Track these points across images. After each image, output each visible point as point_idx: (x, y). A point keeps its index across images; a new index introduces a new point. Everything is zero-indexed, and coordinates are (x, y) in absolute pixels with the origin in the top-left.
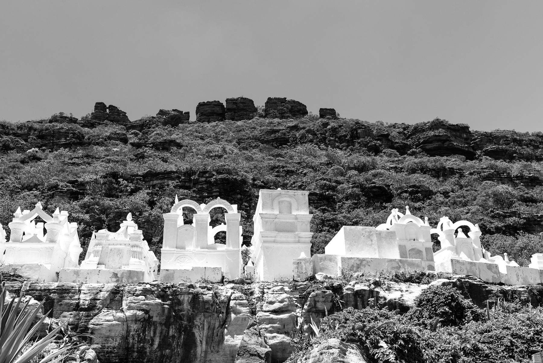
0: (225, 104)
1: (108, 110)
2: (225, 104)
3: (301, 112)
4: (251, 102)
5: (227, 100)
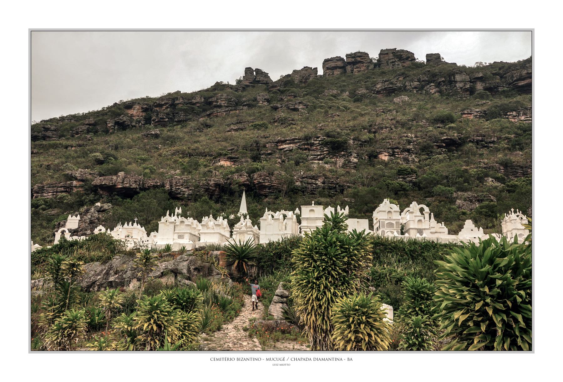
0: (345, 58)
1: (254, 73)
2: (345, 58)
3: (410, 59)
5: (347, 55)
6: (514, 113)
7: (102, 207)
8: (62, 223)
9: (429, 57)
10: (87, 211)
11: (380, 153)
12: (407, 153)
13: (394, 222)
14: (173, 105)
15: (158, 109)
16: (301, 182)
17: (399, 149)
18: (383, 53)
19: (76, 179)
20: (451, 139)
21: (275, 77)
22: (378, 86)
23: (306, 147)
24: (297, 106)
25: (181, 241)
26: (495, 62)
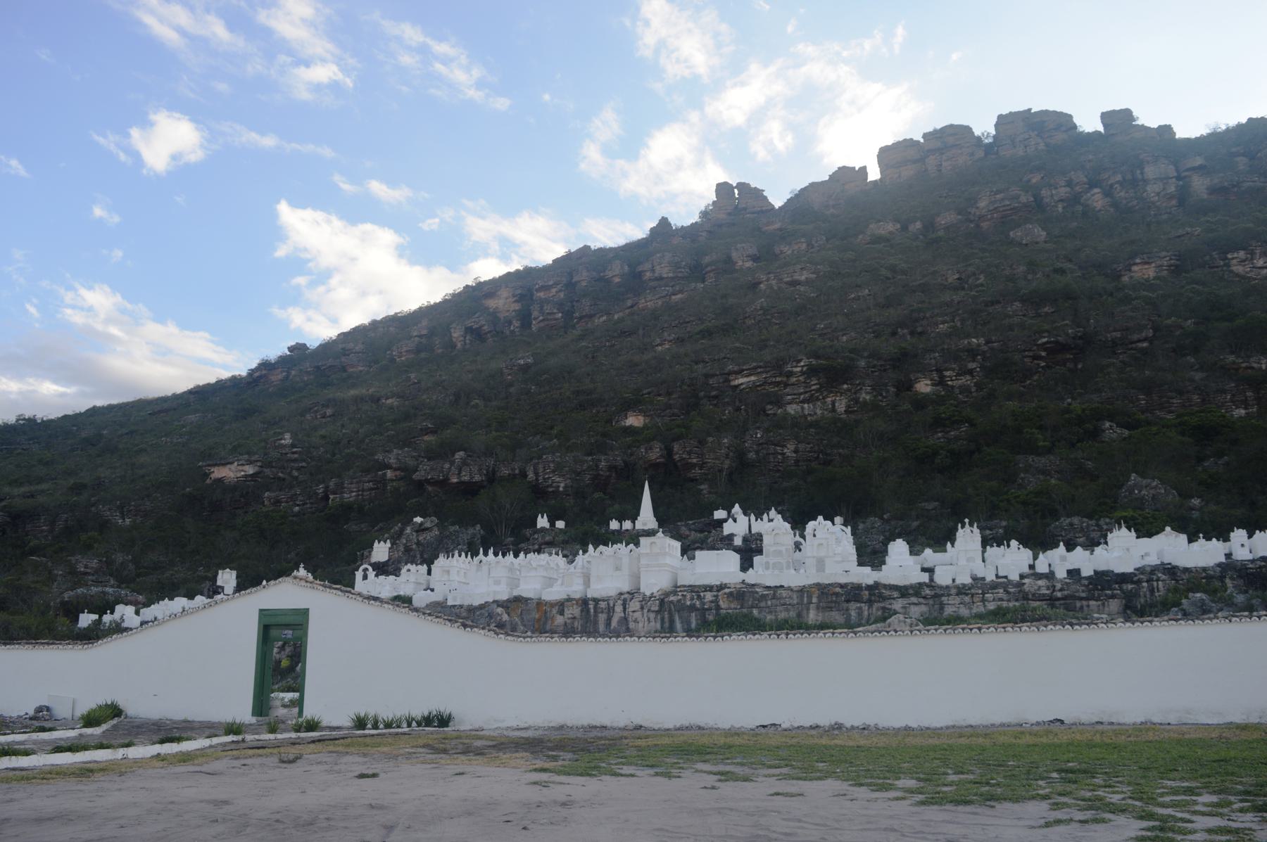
4: (967, 130)
6: (1242, 254)
7: (422, 524)
8: (366, 553)
9: (1107, 117)
10: (400, 533)
11: (917, 380)
12: (968, 377)
13: (783, 549)
14: (570, 285)
15: (541, 294)
16: (757, 452)
17: (953, 370)
18: (1002, 121)
19: (388, 467)
20: (1057, 342)
21: (777, 200)
22: (982, 204)
23: (778, 379)
24: (796, 277)
25: (497, 588)
26: (1250, 119)
